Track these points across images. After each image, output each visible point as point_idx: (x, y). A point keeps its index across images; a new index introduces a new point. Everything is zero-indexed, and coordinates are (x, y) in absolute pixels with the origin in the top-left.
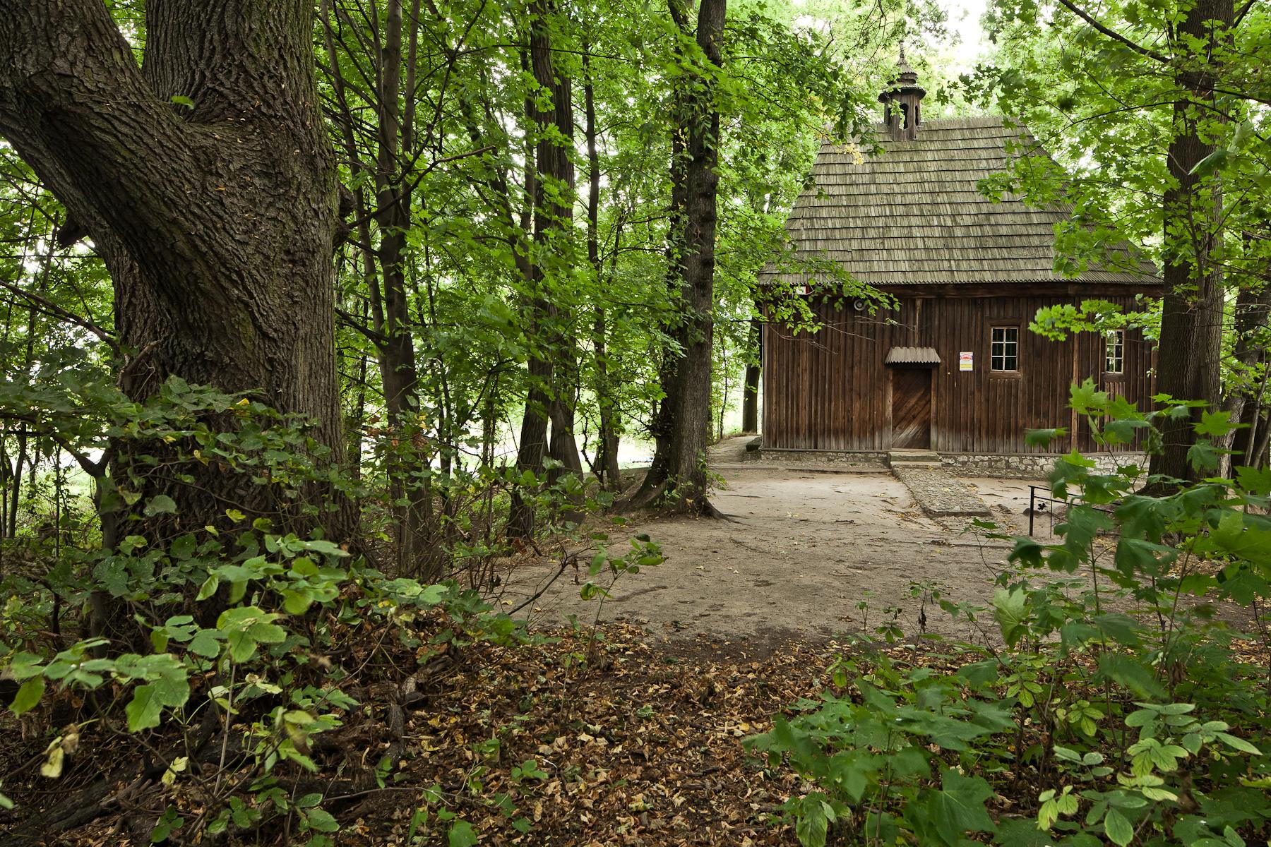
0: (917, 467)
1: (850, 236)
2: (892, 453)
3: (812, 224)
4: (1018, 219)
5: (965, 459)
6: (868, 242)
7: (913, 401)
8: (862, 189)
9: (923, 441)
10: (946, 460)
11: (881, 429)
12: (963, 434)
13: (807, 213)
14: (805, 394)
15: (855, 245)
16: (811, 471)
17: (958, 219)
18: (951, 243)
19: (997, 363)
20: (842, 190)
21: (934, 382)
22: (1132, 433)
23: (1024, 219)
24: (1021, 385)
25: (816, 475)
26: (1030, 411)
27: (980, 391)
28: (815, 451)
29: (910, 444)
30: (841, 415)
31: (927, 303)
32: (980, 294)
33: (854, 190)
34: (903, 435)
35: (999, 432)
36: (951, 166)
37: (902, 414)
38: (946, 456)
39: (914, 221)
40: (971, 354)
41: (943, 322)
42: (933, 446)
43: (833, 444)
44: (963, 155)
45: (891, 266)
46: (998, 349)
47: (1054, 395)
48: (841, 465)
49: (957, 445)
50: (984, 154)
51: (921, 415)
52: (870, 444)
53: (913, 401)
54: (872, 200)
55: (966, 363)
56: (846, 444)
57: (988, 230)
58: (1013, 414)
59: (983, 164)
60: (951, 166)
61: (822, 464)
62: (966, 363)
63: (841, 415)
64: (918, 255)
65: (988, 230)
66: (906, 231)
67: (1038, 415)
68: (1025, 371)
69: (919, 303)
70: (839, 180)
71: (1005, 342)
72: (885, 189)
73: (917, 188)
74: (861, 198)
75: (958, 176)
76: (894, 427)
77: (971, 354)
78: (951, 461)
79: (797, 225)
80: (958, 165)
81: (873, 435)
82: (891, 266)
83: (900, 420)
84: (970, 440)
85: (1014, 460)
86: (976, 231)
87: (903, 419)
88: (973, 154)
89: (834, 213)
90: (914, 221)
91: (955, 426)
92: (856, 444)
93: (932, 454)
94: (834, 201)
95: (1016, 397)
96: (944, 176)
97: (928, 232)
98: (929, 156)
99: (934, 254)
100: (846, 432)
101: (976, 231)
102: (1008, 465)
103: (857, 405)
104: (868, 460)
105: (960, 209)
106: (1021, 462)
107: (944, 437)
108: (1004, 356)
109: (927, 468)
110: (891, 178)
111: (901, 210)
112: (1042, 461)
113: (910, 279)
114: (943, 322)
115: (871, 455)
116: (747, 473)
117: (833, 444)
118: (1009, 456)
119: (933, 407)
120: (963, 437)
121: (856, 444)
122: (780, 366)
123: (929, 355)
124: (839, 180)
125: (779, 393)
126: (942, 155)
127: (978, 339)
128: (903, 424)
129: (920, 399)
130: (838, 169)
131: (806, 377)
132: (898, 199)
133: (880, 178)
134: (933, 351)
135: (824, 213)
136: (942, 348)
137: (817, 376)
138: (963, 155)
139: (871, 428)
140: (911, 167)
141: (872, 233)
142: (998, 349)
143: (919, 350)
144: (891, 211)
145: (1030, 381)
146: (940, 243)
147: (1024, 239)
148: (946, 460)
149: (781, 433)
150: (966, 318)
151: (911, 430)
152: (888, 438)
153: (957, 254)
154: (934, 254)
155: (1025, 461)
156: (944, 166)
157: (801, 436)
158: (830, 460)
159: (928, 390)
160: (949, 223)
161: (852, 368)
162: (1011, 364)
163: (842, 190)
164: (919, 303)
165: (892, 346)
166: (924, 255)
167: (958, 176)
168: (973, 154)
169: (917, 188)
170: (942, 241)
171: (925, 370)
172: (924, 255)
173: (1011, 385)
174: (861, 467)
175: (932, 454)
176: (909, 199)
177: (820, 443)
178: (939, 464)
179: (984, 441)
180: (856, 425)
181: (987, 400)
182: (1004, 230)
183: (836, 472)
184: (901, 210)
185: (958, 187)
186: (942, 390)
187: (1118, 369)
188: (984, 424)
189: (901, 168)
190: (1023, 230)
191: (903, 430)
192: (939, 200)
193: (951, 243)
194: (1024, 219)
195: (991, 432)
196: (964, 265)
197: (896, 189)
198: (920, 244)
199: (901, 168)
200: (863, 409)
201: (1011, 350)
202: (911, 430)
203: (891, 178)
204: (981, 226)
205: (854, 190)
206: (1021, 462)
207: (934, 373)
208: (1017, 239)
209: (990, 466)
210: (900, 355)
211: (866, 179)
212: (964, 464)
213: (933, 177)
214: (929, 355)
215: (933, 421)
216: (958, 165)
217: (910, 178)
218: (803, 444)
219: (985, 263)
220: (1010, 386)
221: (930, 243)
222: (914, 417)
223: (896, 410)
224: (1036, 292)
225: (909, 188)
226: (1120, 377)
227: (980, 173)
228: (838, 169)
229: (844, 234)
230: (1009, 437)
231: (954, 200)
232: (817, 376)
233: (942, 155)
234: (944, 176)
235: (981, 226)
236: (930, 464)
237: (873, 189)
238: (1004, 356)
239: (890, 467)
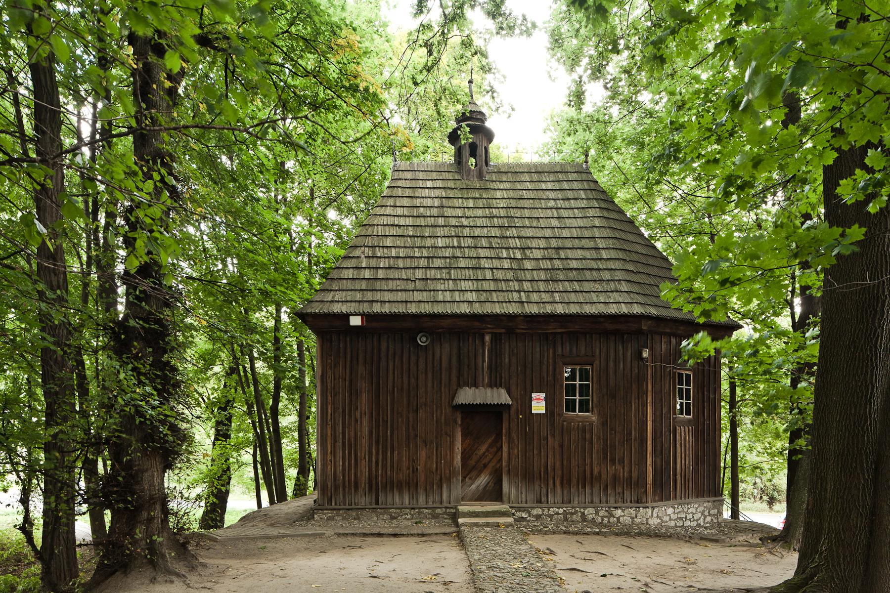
0: (487, 525)
1: (415, 264)
2: (461, 508)
3: (374, 252)
4: (588, 254)
5: (540, 511)
6: (433, 271)
7: (483, 448)
8: (430, 222)
9: (494, 493)
10: (519, 514)
11: (449, 480)
12: (537, 483)
13: (369, 241)
14: (365, 442)
15: (419, 274)
16: (365, 535)
17: (528, 252)
18: (521, 275)
19: (571, 406)
20: (409, 221)
21: (505, 425)
22: (467, 441)
23: (594, 255)
24: (595, 431)
25: (370, 540)
26: (605, 458)
27: (554, 436)
28: (376, 506)
29: (481, 497)
30: (405, 464)
31: (496, 338)
32: (552, 328)
33: (421, 222)
34: (474, 487)
35: (574, 481)
36: (521, 203)
37: (472, 462)
38: (519, 509)
39: (482, 253)
40: (543, 395)
41: (514, 360)
42: (505, 499)
43: (397, 500)
44: (531, 195)
45: (457, 296)
46: (571, 390)
47: (629, 440)
48: (405, 523)
49: (530, 497)
50: (551, 195)
51: (492, 464)
52: (437, 498)
53: (483, 448)
54: (440, 232)
55: (539, 406)
56: (411, 498)
57: (558, 264)
58: (588, 461)
59: (552, 204)
60: (521, 203)
61: (383, 524)
62: (539, 406)
63: (405, 464)
64: (486, 285)
65: (558, 264)
66: (474, 262)
67: (613, 461)
68: (599, 414)
69: (487, 338)
70: (406, 212)
71: (578, 382)
72: (453, 222)
73: (486, 222)
74: (428, 229)
75: (527, 213)
76: (464, 478)
77: (543, 395)
78: (524, 515)
79: (357, 252)
80: (527, 204)
81: (440, 487)
82: (457, 296)
83: (470, 470)
84: (544, 491)
85: (590, 512)
86: (547, 264)
87: (473, 468)
88: (541, 194)
89: (398, 242)
90: (482, 253)
91: (528, 475)
92: (422, 498)
93: (504, 507)
94: (400, 231)
95: (591, 442)
96: (512, 212)
97: (496, 263)
98: (499, 194)
99: (503, 286)
100: (411, 485)
101: (547, 264)
102: (584, 518)
103: (423, 453)
104: (435, 517)
105: (529, 243)
106: (597, 513)
107: (517, 488)
108: (577, 398)
109: (498, 525)
110: (459, 213)
111: (469, 242)
112: (619, 512)
113: (478, 309)
114: (514, 360)
115: (438, 511)
116: (280, 544)
117: (397, 500)
118: (585, 508)
119: (505, 455)
120: (537, 487)
121: (422, 498)
122: (335, 410)
123: (501, 397)
124: (406, 212)
125: (335, 441)
126: (512, 194)
127: (550, 378)
128: (474, 473)
129: (490, 446)
130: (406, 202)
131: (365, 422)
132: (467, 232)
133: (448, 212)
134: (503, 392)
135: (388, 242)
136: (513, 388)
137: (377, 421)
138: (531, 195)
139: (439, 479)
140: (480, 203)
141: (438, 263)
142: (571, 390)
143: (489, 391)
144: (459, 242)
145: (604, 424)
146: (509, 275)
147: (594, 273)
148: (519, 514)
149: (336, 488)
150: (538, 355)
151: (483, 480)
152: (457, 490)
153: (527, 286)
154: (503, 286)
155: (602, 513)
156: (513, 203)
157: (360, 490)
158: (393, 518)
159: (499, 435)
160: (519, 256)
161: (417, 411)
162: (584, 407)
163: (409, 221)
164: (487, 338)
165: (459, 386)
166: (492, 286)
167: (527, 213)
168: (541, 194)
169: (486, 222)
170: (512, 273)
171: (496, 412)
172: (492, 286)
173: (585, 429)
174: (428, 526)
175: (504, 507)
176: (477, 232)
177: (382, 499)
178: (510, 520)
179: (559, 491)
180: (422, 477)
181: (561, 446)
182: (574, 264)
183: (395, 535)
184: (469, 242)
185: (527, 223)
186: (514, 435)
187: (688, 413)
188: (559, 473)
189: (471, 203)
190: (593, 264)
191: (473, 480)
192: (508, 234)
193: (521, 275)
194: (594, 255)
195: (566, 482)
196: (535, 297)
197: (465, 222)
198: (488, 274)
199: (471, 203)
200: (429, 457)
201: (584, 390)
202: (483, 480)
203: (459, 213)
204: (551, 259)
205: (421, 222)
206: (597, 513)
207: (505, 416)
208: (587, 273)
209: (566, 519)
210: (467, 396)
211: (435, 212)
212: (538, 517)
213: (503, 213)
214: (499, 396)
215: (505, 470)
216: (527, 204)
217: (480, 213)
218: (363, 500)
219: (556, 295)
220: (584, 430)
221: (500, 275)
222: (485, 466)
223: (464, 459)
224: (610, 327)
225: (479, 222)
226: (689, 420)
227: (549, 211)
228: (406, 202)
229: (408, 263)
230: (584, 487)
231: (523, 234)
232: (377, 421)
233: (512, 194)
234: (512, 212)
235: (551, 259)
236: (502, 520)
237: (441, 221)
238: (577, 398)
239: (457, 525)
